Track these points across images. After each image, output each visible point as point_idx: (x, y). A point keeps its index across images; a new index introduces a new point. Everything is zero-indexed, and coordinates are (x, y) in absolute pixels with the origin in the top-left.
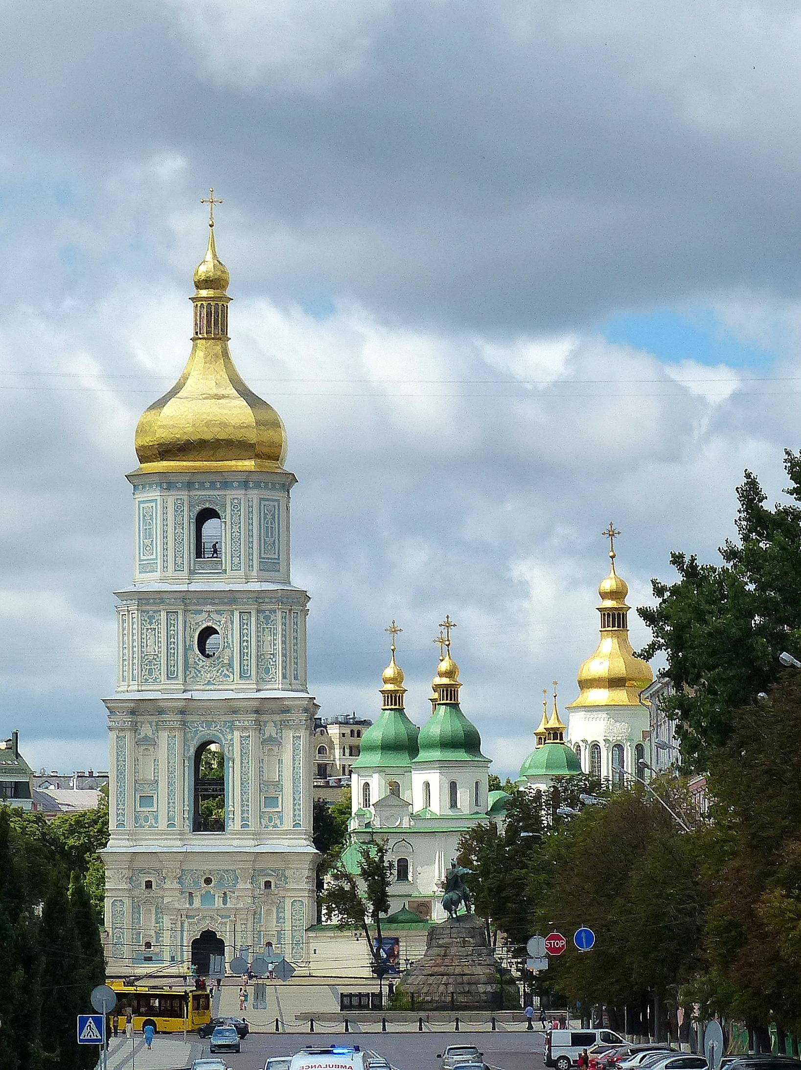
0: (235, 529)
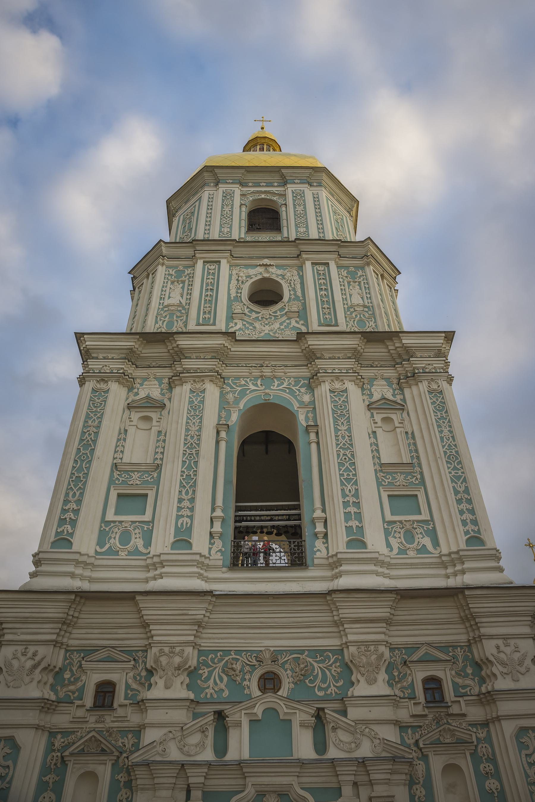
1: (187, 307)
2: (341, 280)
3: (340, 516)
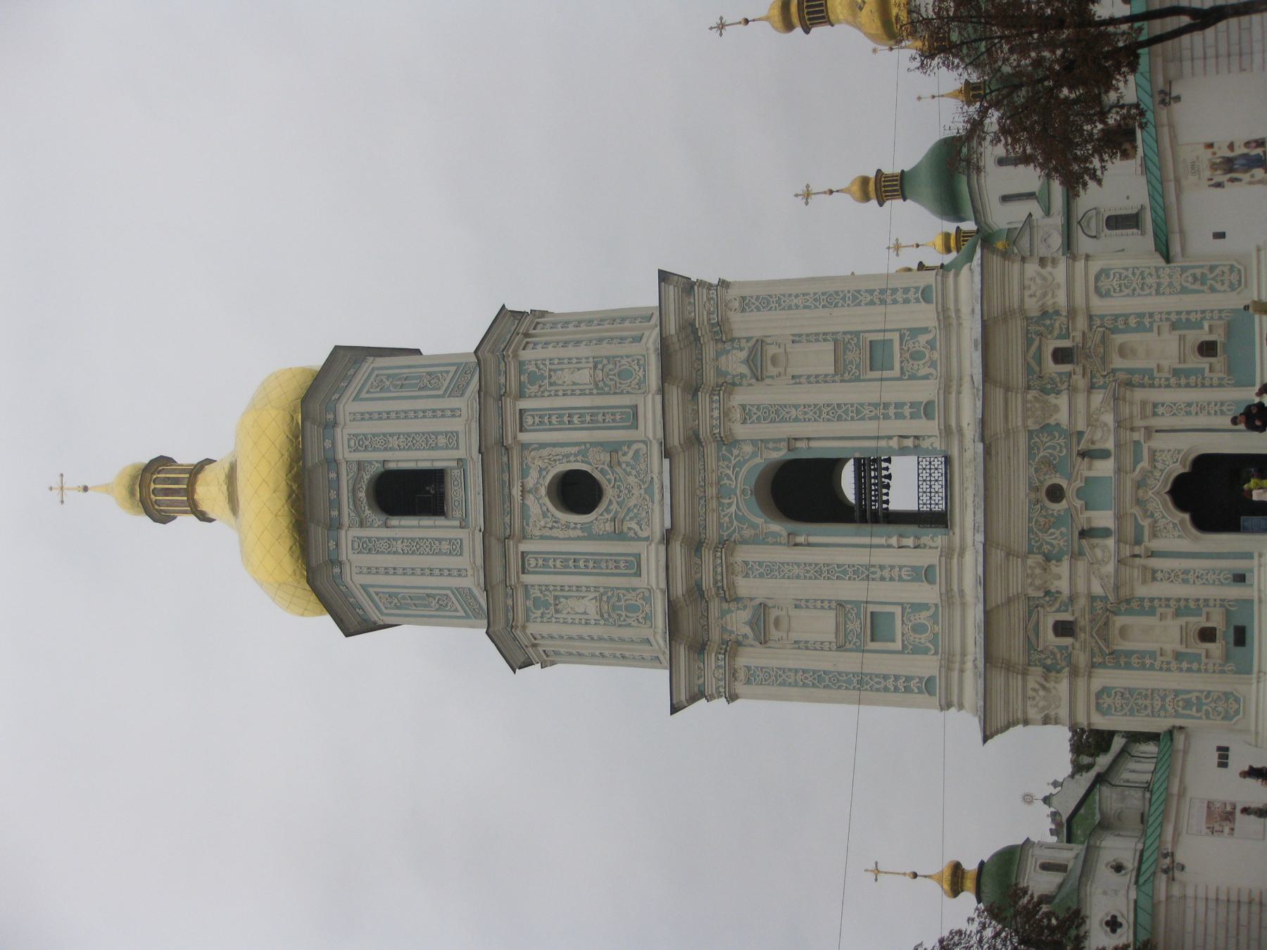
0: (394, 442)
1: (602, 590)
2: (546, 394)
3: (900, 423)
